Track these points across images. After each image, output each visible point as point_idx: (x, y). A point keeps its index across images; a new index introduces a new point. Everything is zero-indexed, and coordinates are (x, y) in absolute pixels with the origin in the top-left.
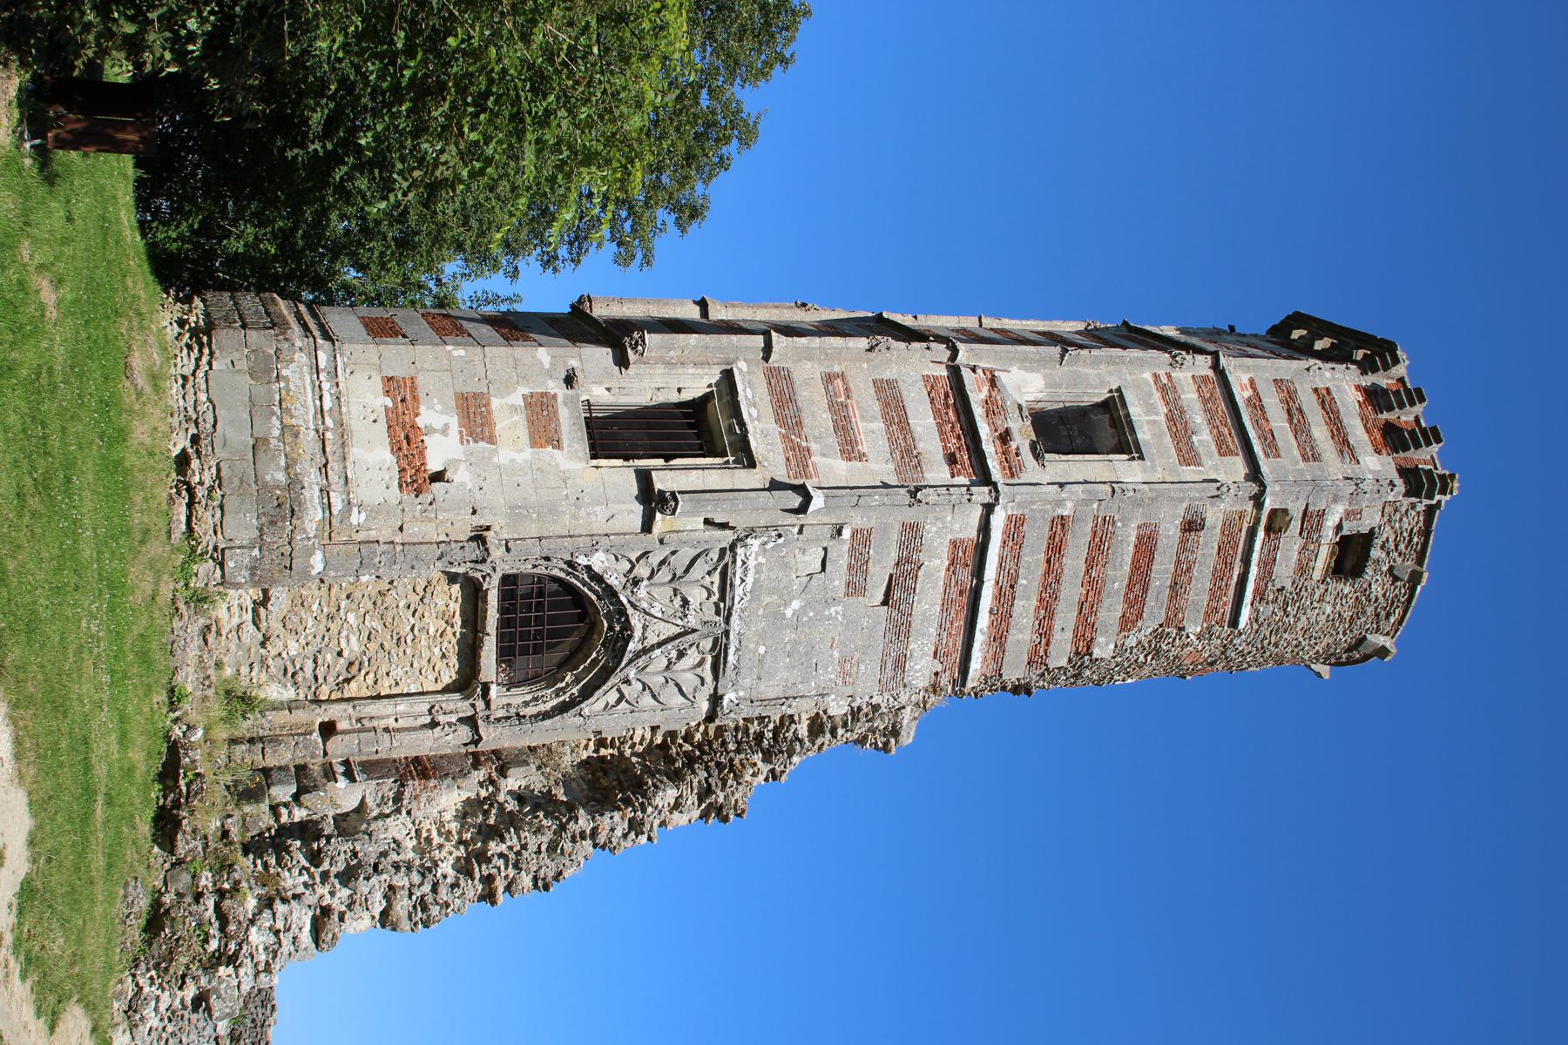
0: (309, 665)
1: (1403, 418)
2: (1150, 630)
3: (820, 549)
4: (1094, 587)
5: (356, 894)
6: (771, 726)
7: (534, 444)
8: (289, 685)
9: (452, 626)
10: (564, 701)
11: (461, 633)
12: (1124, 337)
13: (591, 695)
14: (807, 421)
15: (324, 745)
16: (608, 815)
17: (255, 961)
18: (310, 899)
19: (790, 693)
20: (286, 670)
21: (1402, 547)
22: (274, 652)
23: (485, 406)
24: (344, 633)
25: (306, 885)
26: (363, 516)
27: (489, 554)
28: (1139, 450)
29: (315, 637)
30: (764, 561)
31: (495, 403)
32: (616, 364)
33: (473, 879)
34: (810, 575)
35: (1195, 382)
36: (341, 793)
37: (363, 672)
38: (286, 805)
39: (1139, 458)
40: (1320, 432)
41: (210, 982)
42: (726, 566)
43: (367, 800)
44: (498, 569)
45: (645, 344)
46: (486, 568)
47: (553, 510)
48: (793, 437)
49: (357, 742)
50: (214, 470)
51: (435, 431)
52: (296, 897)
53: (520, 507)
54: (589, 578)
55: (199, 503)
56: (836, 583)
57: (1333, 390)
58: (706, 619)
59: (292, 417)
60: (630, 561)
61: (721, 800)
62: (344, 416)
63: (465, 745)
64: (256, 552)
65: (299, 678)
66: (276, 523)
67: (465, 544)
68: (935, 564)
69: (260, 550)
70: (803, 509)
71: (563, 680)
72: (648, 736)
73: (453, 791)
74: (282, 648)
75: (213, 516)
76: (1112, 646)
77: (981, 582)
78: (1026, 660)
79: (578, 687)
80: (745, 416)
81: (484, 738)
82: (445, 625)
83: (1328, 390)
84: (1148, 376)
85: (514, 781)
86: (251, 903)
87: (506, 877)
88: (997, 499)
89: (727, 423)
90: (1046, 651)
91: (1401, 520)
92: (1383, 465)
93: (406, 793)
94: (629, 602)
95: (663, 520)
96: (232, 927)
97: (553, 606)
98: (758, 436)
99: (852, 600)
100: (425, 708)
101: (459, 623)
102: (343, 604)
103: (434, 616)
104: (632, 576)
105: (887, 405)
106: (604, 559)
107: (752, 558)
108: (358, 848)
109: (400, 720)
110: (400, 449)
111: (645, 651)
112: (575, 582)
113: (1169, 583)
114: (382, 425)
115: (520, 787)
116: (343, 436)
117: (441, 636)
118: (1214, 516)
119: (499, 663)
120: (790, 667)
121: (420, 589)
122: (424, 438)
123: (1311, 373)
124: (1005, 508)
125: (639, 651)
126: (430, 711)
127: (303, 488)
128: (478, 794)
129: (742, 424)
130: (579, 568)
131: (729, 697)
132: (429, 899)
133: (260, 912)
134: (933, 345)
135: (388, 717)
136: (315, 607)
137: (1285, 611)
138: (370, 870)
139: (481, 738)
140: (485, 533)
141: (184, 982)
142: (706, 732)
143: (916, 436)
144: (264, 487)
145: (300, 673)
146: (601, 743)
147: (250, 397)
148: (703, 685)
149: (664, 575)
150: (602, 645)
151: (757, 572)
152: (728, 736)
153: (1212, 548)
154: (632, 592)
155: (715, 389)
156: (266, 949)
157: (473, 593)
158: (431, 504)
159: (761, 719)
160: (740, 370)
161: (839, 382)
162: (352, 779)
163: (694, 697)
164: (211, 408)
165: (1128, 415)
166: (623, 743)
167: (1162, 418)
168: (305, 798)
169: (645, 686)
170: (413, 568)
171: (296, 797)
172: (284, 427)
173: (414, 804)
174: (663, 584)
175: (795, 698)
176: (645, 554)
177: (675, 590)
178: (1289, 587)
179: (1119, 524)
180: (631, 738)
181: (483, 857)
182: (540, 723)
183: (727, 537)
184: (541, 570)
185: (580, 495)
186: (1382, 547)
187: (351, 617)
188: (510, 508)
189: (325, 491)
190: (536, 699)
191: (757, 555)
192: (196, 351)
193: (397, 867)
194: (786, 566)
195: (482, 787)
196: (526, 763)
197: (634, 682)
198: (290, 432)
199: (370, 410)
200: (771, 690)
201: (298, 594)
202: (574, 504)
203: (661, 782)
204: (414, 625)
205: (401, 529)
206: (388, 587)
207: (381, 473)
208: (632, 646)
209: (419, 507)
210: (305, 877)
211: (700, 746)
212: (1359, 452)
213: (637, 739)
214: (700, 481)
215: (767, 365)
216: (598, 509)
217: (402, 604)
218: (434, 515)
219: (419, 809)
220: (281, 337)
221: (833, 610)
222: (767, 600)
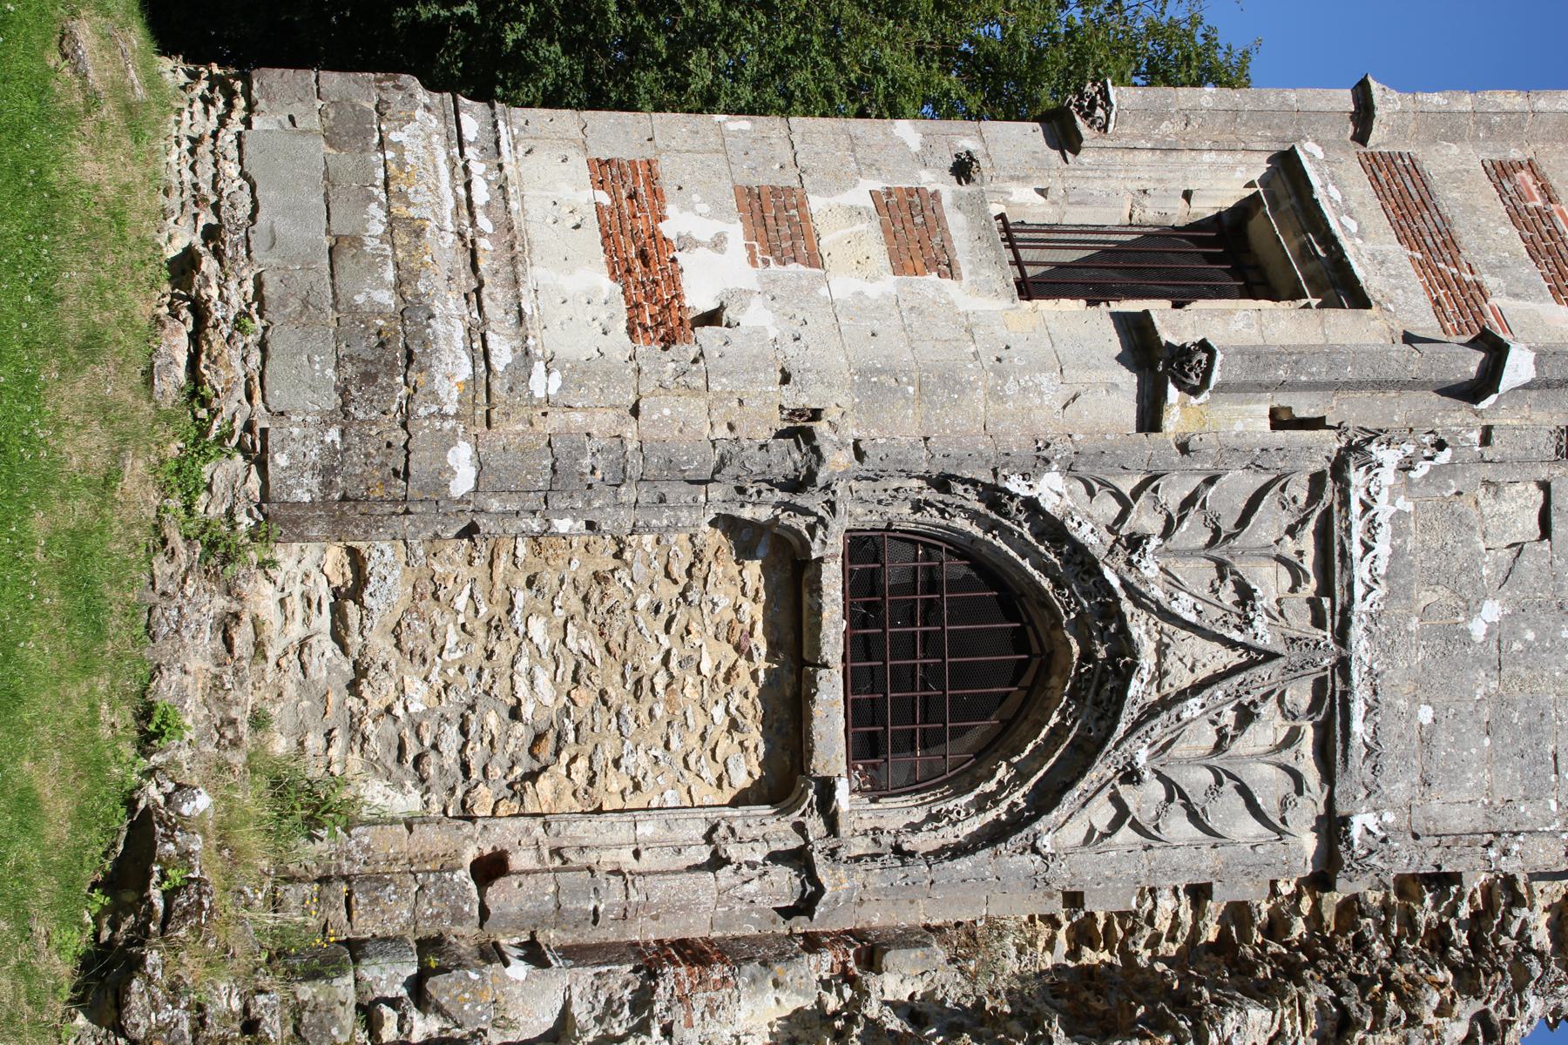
0: (451, 739)
3: (1533, 487)
6: (1465, 911)
7: (899, 268)
8: (409, 784)
9: (750, 658)
10: (997, 821)
11: (767, 671)
13: (1055, 802)
15: (482, 894)
19: (1500, 822)
20: (401, 748)
22: (376, 705)
24: (523, 664)
26: (556, 380)
27: (820, 459)
29: (461, 669)
30: (1408, 506)
31: (816, 203)
32: (1053, 147)
34: (1518, 548)
36: (517, 991)
37: (565, 757)
38: (394, 1003)
42: (1328, 513)
45: (1109, 103)
46: (812, 500)
47: (950, 381)
48: (1442, 265)
49: (552, 888)
50: (249, 287)
51: (697, 244)
54: (1036, 536)
55: (215, 327)
58: (1295, 634)
60: (1118, 495)
62: (514, 216)
63: (787, 913)
66: (375, 377)
69: (343, 434)
71: (992, 775)
72: (1186, 916)
73: (763, 991)
74: (393, 695)
75: (244, 359)
79: (1025, 789)
81: (829, 889)
82: (734, 655)
89: (1295, 243)
93: (660, 990)
94: (1125, 585)
95: (1184, 405)
97: (962, 611)
98: (1365, 260)
100: (700, 829)
101: (764, 650)
102: (520, 600)
103: (711, 631)
104: (1124, 531)
106: (1065, 491)
107: (1383, 499)
109: (644, 854)
110: (629, 271)
111: (1165, 704)
114: (592, 233)
115: (912, 996)
116: (512, 247)
117: (727, 680)
120: (1492, 760)
121: (678, 570)
125: (1154, 705)
126: (708, 838)
127: (432, 316)
128: (820, 1002)
129: (1329, 240)
130: (1013, 506)
131: (1362, 822)
135: (619, 846)
136: (462, 602)
142: (1315, 918)
144: (350, 316)
145: (433, 756)
146: (1083, 934)
147: (327, 172)
148: (1299, 791)
149: (1193, 532)
150: (1072, 695)
154: (1129, 562)
155: (1261, 190)
159: (1442, 881)
160: (1311, 156)
161: (1524, 176)
164: (247, 188)
166: (1131, 932)
169: (1172, 790)
171: (417, 988)
172: (392, 221)
173: (679, 1012)
174: (1192, 553)
176: (1150, 481)
177: (1221, 566)
180: (1150, 920)
182: (947, 863)
183: (1330, 442)
185: (1004, 354)
187: (537, 628)
188: (860, 372)
192: (220, 104)
197: (1147, 775)
201: (426, 573)
203: (1233, 998)
204: (668, 652)
205: (635, 411)
206: (612, 564)
208: (1135, 688)
209: (673, 365)
211: (1304, 946)
213: (1163, 925)
214: (1254, 331)
215: (1362, 150)
216: (1043, 379)
217: (642, 603)
218: (701, 382)
219: (690, 1025)
220: (389, 84)
222: (1426, 597)
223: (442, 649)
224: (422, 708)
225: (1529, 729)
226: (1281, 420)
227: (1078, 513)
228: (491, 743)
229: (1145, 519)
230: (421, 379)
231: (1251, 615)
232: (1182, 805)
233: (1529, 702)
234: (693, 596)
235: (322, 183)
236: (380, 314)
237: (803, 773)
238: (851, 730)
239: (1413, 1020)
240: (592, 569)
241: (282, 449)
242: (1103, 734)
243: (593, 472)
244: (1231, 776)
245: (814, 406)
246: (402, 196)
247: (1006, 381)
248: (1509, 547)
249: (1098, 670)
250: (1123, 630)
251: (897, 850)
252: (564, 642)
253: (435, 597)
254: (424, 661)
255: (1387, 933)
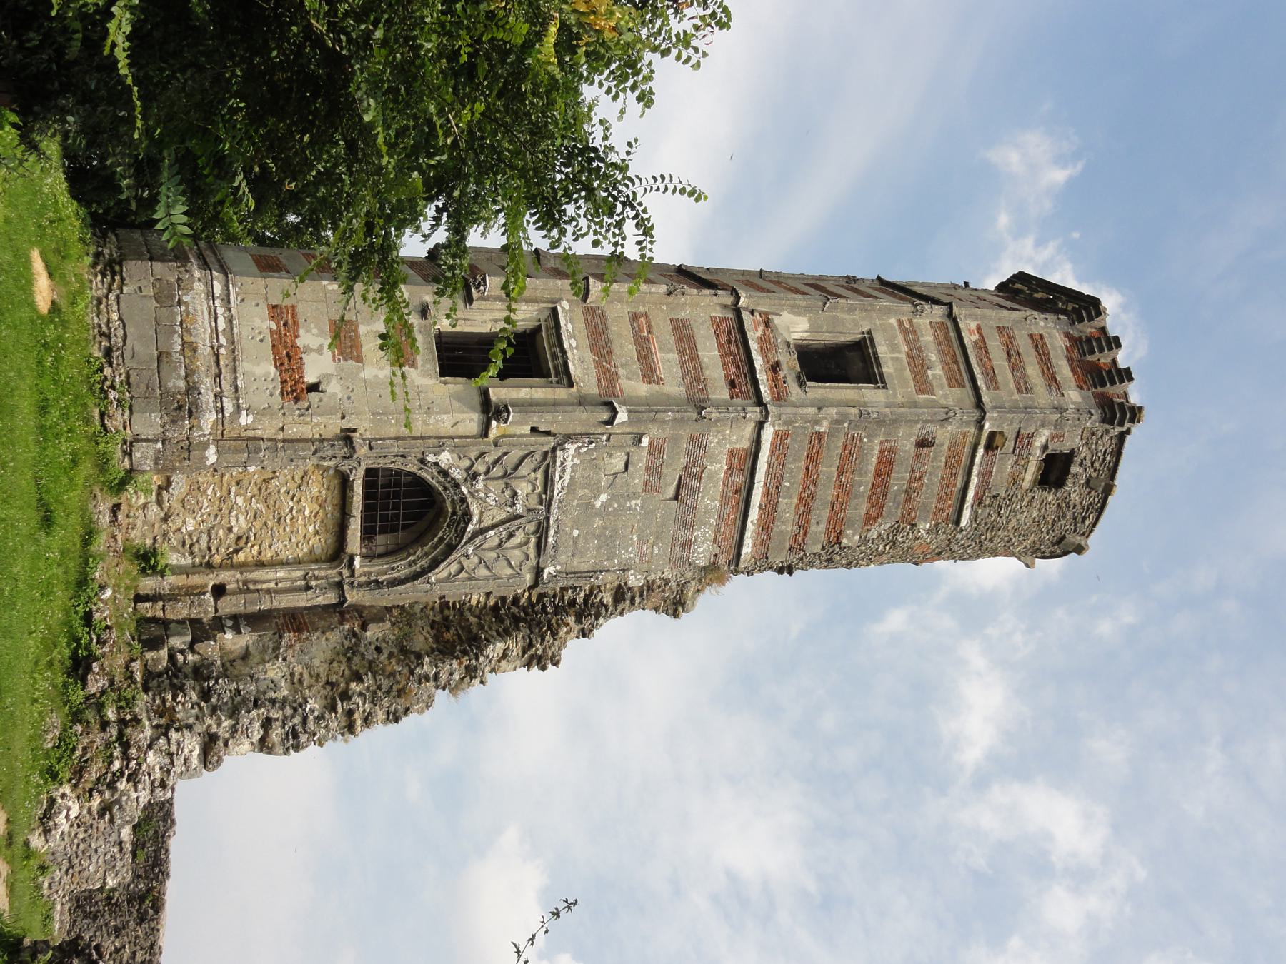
0: (205, 538)
1: (1102, 361)
2: (889, 525)
4: (845, 494)
5: (238, 724)
6: (582, 594)
12: (876, 289)
13: (437, 566)
14: (616, 350)
15: (216, 603)
16: (448, 661)
17: (152, 778)
18: (199, 728)
19: (598, 567)
21: (1097, 464)
22: (174, 528)
23: (353, 331)
24: (234, 513)
25: (197, 718)
26: (251, 418)
28: (883, 381)
30: (578, 462)
31: (362, 329)
33: (336, 713)
34: (616, 474)
35: (932, 327)
37: (249, 545)
38: (182, 652)
39: (884, 388)
40: (1033, 370)
41: (113, 796)
42: (548, 465)
43: (251, 649)
45: (486, 285)
48: (604, 364)
50: (123, 377)
51: (312, 350)
52: (189, 727)
53: (380, 414)
56: (637, 481)
57: (1046, 336)
58: (531, 507)
59: (191, 335)
61: (540, 652)
64: (160, 445)
65: (196, 549)
66: (177, 422)
67: (336, 443)
68: (718, 467)
69: (163, 444)
70: (610, 422)
71: (415, 553)
72: (482, 599)
75: (123, 415)
76: (857, 537)
77: (752, 483)
78: (788, 546)
80: (566, 346)
83: (1041, 337)
84: (893, 321)
85: (373, 632)
86: (148, 732)
87: (364, 711)
88: (767, 418)
90: (804, 540)
91: (1097, 443)
92: (1083, 398)
94: (469, 492)
95: (498, 427)
96: (133, 751)
98: (576, 362)
100: (300, 573)
102: (233, 489)
103: (309, 500)
105: (681, 339)
106: (450, 458)
108: (241, 687)
110: (282, 364)
111: (482, 531)
112: (424, 475)
113: (905, 488)
116: (234, 352)
117: (315, 516)
118: (943, 435)
119: (363, 539)
121: (297, 478)
122: (303, 356)
123: (1028, 322)
124: (773, 425)
126: (305, 578)
129: (563, 352)
130: (429, 465)
131: (549, 570)
132: (300, 729)
133: (158, 739)
134: (719, 292)
136: (210, 491)
137: (999, 513)
138: (251, 705)
139: (345, 600)
140: (352, 434)
141: (91, 796)
143: (704, 365)
144: (165, 393)
145: (197, 545)
148: (528, 560)
149: (497, 471)
151: (573, 471)
152: (547, 601)
153: (940, 461)
154: (472, 484)
156: (161, 768)
157: (345, 483)
158: (307, 409)
159: (574, 588)
160: (563, 308)
161: (643, 320)
162: (239, 632)
165: (875, 353)
167: (903, 356)
168: (199, 647)
170: (292, 460)
172: (184, 343)
175: (601, 572)
176: (482, 454)
178: (1003, 494)
179: (865, 440)
181: (345, 696)
183: (550, 442)
184: (398, 466)
185: (431, 406)
186: (1081, 465)
187: (240, 500)
188: (373, 414)
189: (219, 396)
190: (393, 569)
191: (573, 457)
193: (273, 702)
194: (596, 467)
195: (346, 638)
196: (382, 620)
198: (189, 348)
199: (257, 331)
200: (581, 564)
202: (426, 413)
205: (282, 429)
206: (272, 475)
207: (266, 383)
208: (470, 528)
209: (298, 412)
210: (196, 710)
211: (524, 609)
212: (1064, 386)
215: (584, 305)
216: (445, 417)
217: (283, 490)
218: (309, 419)
220: (182, 269)
221: (633, 503)
223: (201, 508)
224: (193, 528)
225: (611, 537)
226: (534, 430)
228: (221, 540)
229: (480, 467)
230: (195, 422)
234: (303, 488)
235: (154, 323)
236: (179, 393)
240: (263, 478)
241: (138, 451)
244: (503, 556)
246: (188, 330)
247: (430, 417)
248: (613, 474)
250: (468, 506)
251: (376, 581)
252: (250, 504)
253: (199, 488)
254: (194, 512)
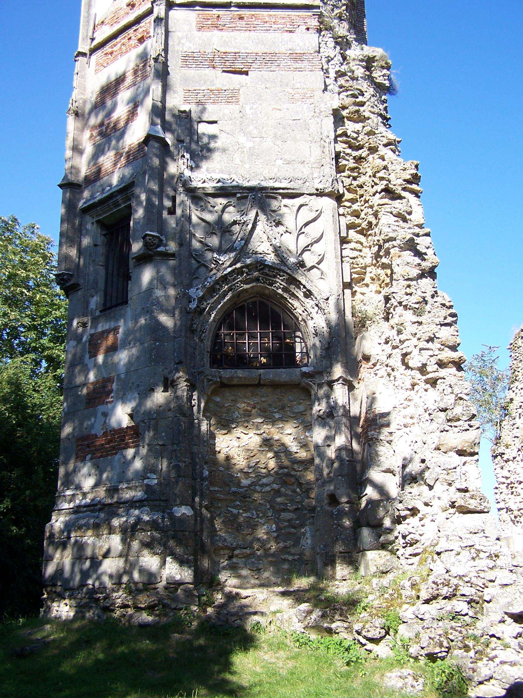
6: (349, 151)
17: (486, 569)
37: (293, 473)
44: (200, 370)
49: (340, 477)
56: (227, 112)
94: (230, 266)
99: (242, 99)
102: (233, 489)
136: (235, 511)
163: (317, 211)
181: (423, 369)
185: (146, 310)
213: (355, 254)
227: (204, 283)
231: (242, 221)
232: (311, 246)
233: (275, 128)
237: (299, 384)
238: (284, 366)
239: (385, 168)
242: (285, 275)
243: (185, 462)
245: (163, 379)
249: (262, 276)
255: (357, 177)
